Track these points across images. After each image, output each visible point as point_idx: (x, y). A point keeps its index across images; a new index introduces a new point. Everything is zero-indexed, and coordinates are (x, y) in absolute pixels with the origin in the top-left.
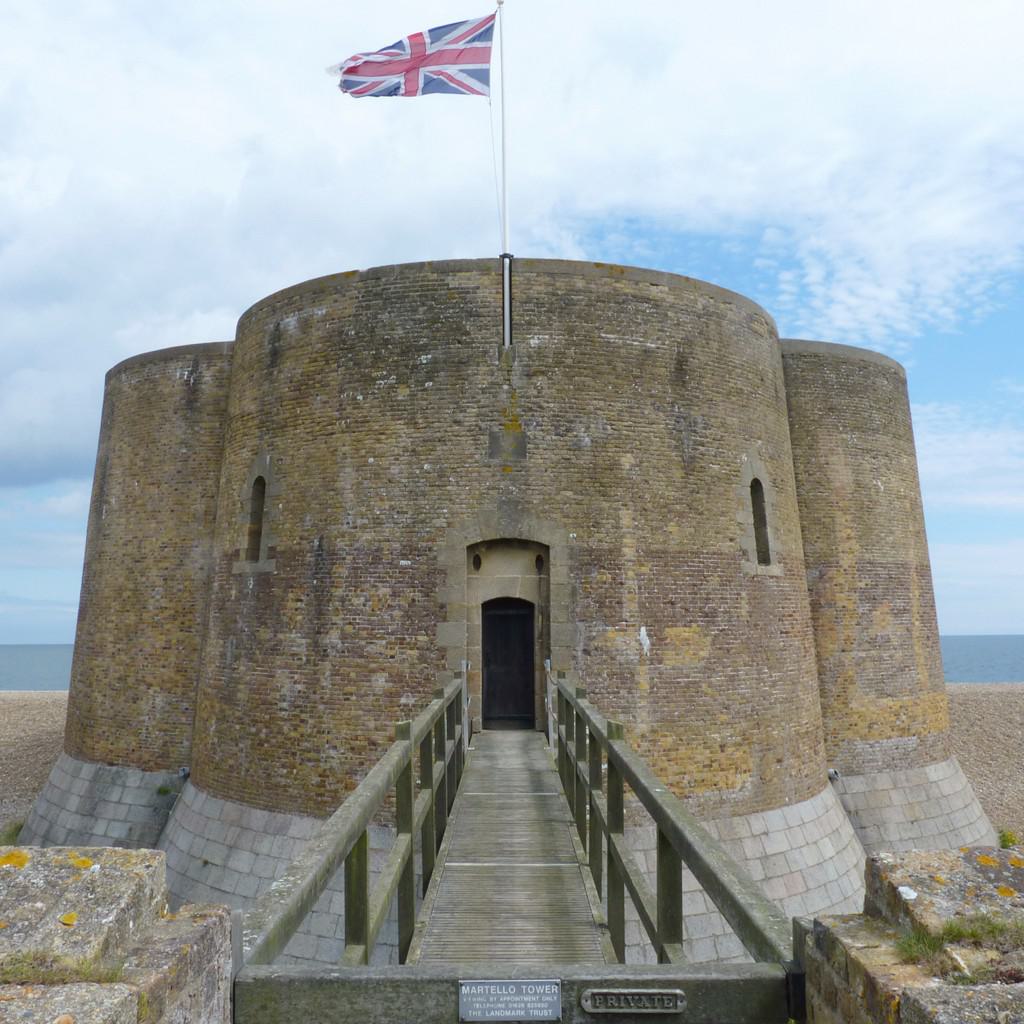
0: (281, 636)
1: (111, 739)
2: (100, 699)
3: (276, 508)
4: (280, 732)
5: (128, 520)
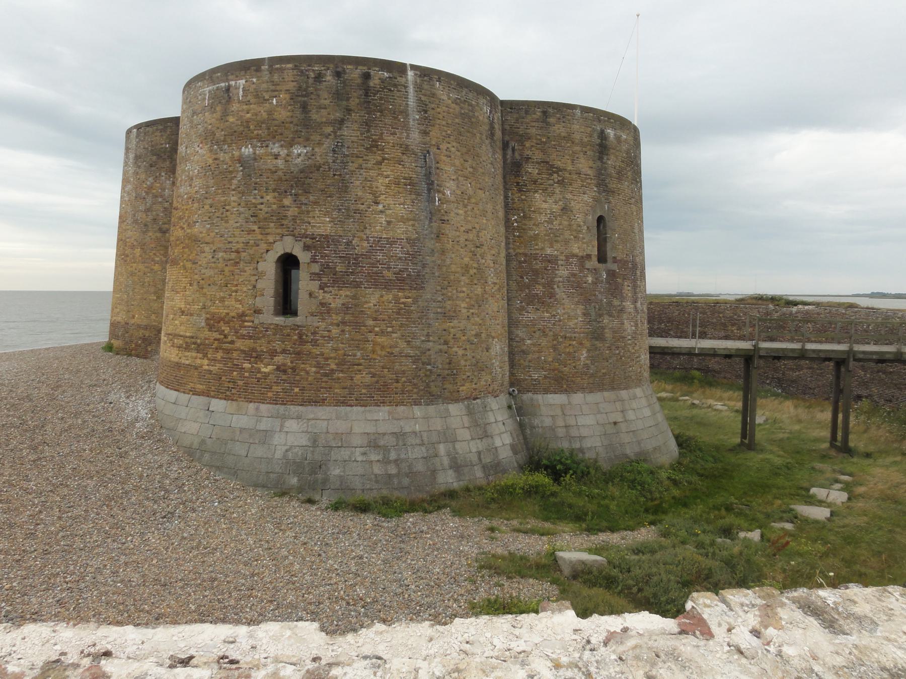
0: (624, 303)
1: (475, 380)
2: (461, 352)
3: (614, 236)
4: (629, 351)
5: (466, 212)
